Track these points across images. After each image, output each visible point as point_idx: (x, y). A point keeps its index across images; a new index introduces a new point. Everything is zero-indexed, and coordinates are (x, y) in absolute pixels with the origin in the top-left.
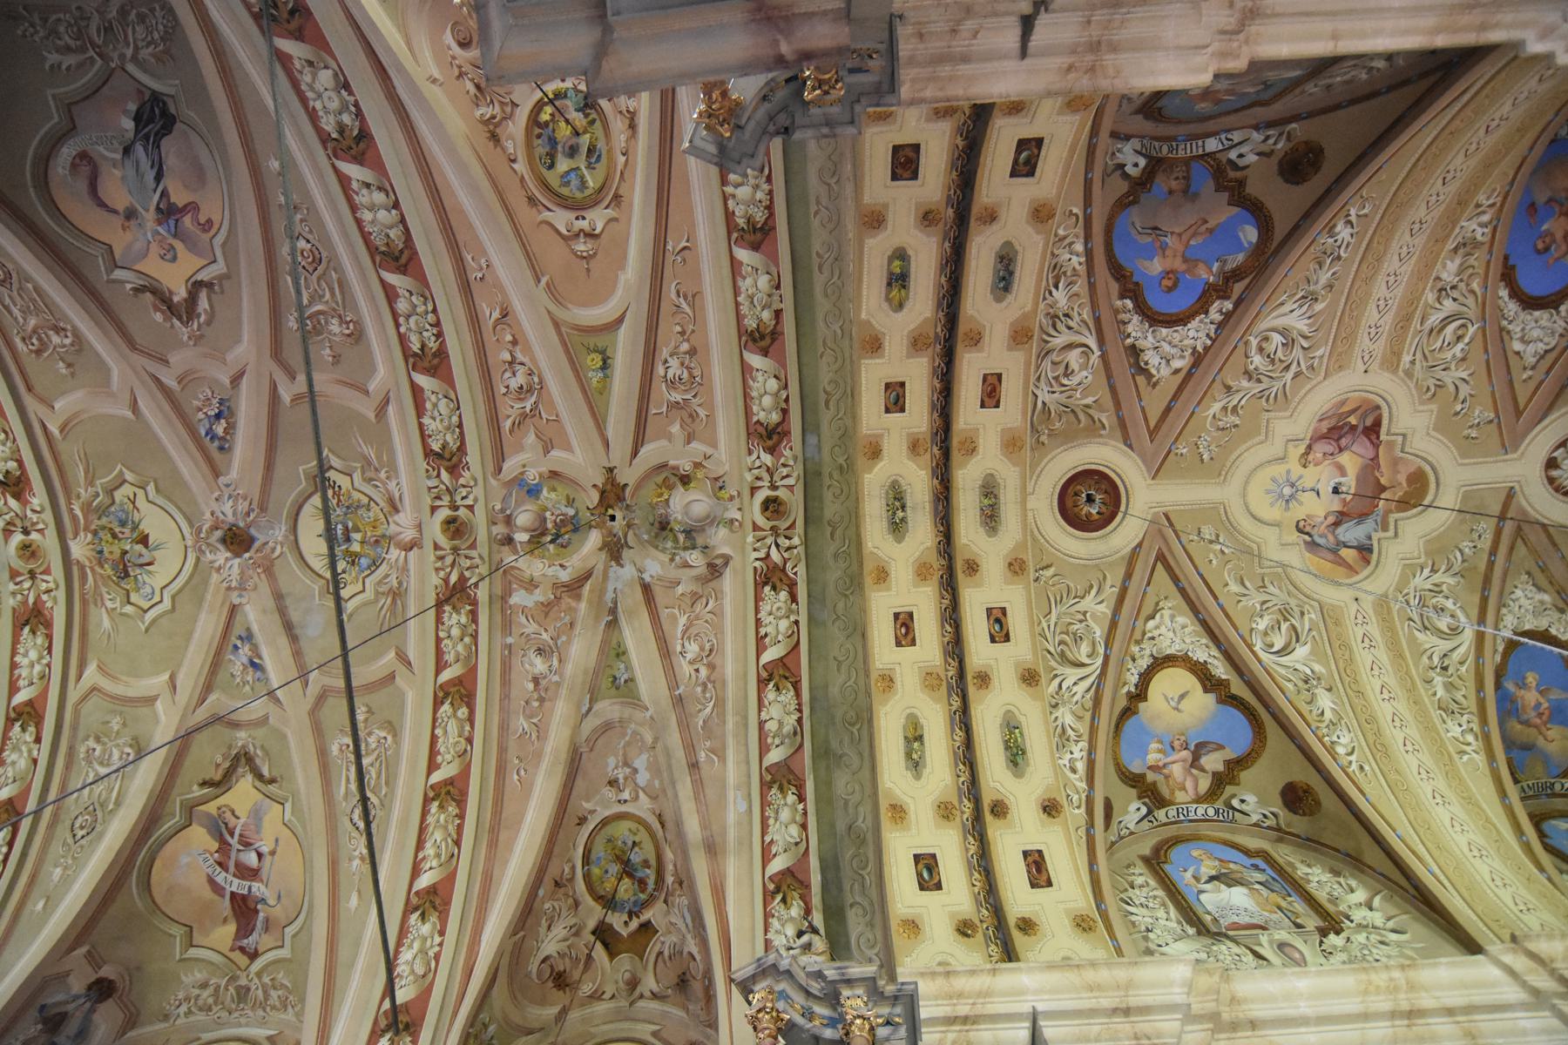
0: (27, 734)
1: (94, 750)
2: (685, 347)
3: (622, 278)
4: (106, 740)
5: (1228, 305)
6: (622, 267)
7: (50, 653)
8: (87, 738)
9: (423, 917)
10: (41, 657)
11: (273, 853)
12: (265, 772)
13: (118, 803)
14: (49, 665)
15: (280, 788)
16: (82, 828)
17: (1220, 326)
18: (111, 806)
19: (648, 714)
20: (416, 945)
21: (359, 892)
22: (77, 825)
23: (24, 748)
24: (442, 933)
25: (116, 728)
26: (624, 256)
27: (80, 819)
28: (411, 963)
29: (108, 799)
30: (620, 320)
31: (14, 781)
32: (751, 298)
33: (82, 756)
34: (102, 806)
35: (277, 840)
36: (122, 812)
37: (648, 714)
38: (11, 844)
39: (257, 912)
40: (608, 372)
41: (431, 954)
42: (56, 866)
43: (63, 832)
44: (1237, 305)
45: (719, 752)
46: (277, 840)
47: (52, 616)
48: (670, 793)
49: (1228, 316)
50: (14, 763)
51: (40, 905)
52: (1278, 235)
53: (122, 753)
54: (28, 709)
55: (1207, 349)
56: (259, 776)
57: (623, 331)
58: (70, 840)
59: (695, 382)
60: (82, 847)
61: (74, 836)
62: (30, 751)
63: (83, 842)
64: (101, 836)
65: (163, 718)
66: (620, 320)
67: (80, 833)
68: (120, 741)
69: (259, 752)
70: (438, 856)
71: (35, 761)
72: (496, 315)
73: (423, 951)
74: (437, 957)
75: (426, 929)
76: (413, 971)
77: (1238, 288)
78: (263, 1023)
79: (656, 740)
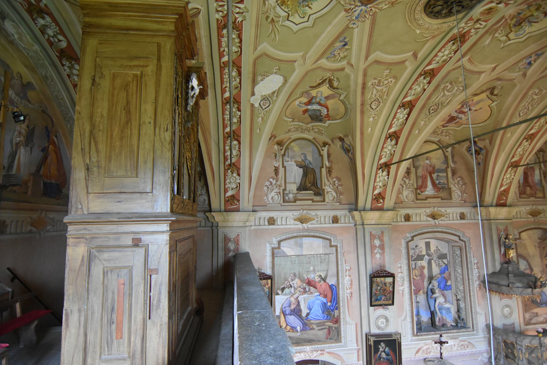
0: (425, 80)
1: (448, 86)
4: (454, 84)
7: (455, 53)
8: (447, 82)
9: (527, 141)
10: (450, 54)
11: (476, 110)
12: (495, 93)
13: (448, 104)
14: (451, 58)
15: (497, 98)
16: (433, 110)
18: (445, 104)
20: (522, 148)
22: (431, 109)
23: (422, 85)
24: (530, 145)
25: (460, 80)
27: (433, 107)
28: (520, 152)
29: (445, 102)
31: (414, 95)
33: (441, 88)
34: (442, 104)
35: (481, 108)
36: (449, 106)
38: (409, 115)
39: (456, 120)
41: (525, 150)
42: (422, 121)
43: (426, 111)
46: (481, 108)
47: (469, 38)
50: (415, 89)
51: (417, 132)
53: (458, 89)
54: (431, 72)
56: (492, 93)
58: (428, 114)
60: (432, 116)
61: (429, 112)
62: (424, 86)
63: (432, 114)
64: (439, 113)
65: (481, 79)
67: (432, 112)
68: (460, 85)
69: (499, 87)
70: (539, 126)
71: (425, 90)
73: (523, 149)
74: (526, 151)
75: (526, 144)
76: (519, 153)
78: (435, 137)
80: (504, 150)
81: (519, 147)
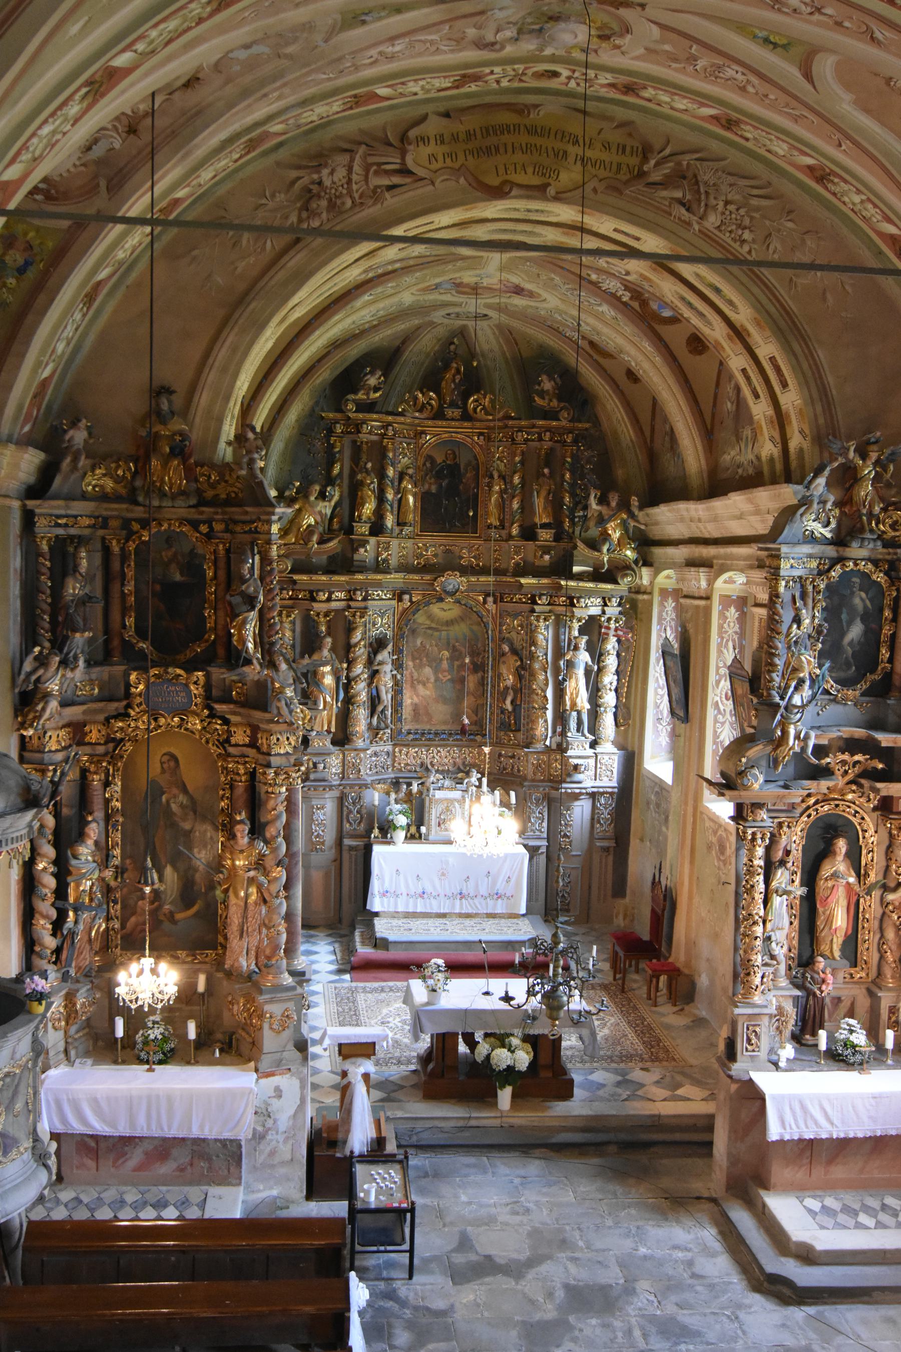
2: (750, 89)
3: (847, 97)
5: (625, 299)
6: (855, 102)
17: (613, 295)
19: (321, 43)
21: (90, 18)
26: (867, 111)
30: (808, 76)
32: (770, 140)
37: (321, 43)
40: (761, 41)
44: (625, 304)
45: (279, 98)
48: (230, 90)
49: (619, 299)
52: (660, 328)
55: (600, 288)
57: (795, 72)
59: (713, 74)
66: (808, 76)
72: (878, 34)
77: (636, 305)
79: (290, 57)
80: (16, 102)
81: (53, 114)
